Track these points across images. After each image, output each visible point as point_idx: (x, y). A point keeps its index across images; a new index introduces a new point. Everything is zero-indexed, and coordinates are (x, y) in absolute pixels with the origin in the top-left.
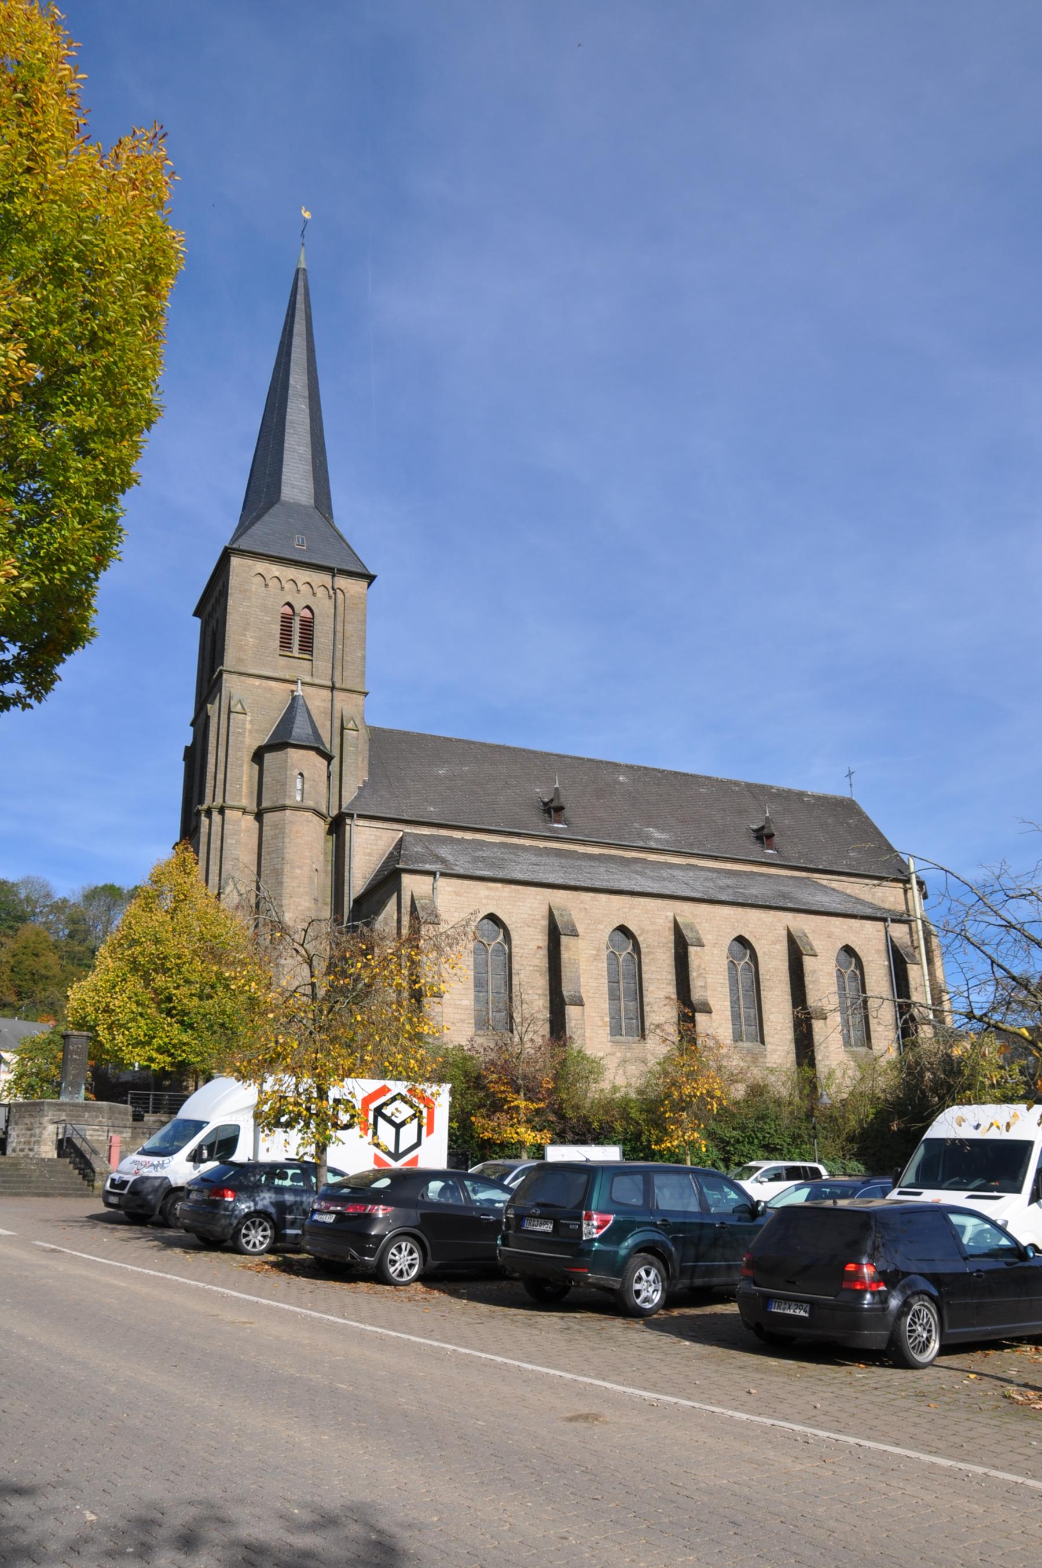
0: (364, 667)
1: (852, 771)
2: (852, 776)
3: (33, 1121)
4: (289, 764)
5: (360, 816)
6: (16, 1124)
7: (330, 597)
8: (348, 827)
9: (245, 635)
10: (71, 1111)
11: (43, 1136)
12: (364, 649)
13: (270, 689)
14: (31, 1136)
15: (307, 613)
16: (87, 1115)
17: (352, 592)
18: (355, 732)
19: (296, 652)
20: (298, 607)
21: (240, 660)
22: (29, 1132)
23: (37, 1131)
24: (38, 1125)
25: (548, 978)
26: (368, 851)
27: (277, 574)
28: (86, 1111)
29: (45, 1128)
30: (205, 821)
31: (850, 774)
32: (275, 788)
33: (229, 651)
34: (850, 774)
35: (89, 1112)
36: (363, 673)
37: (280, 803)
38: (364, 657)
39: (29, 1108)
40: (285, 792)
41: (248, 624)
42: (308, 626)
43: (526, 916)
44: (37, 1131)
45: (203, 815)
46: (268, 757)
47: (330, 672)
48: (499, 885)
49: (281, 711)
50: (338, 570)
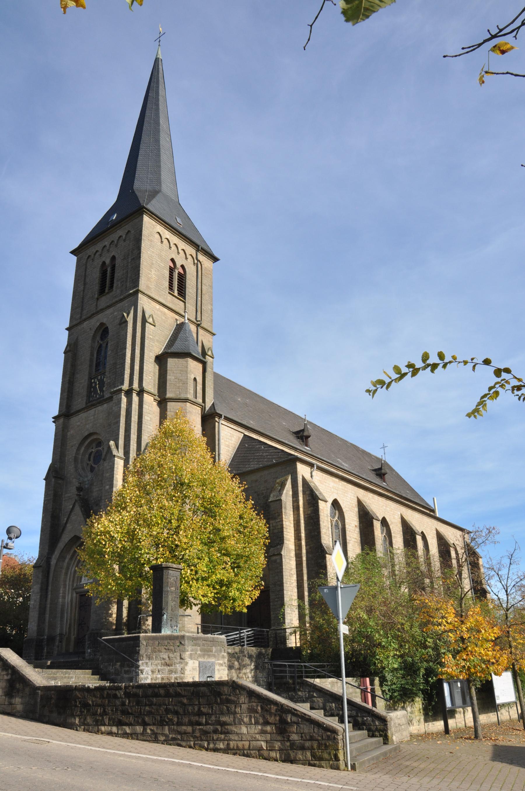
0: (212, 316)
1: (385, 445)
2: (386, 449)
3: (171, 655)
4: (189, 370)
5: (227, 419)
6: (149, 658)
7: (194, 264)
8: (217, 424)
9: (151, 271)
10: (204, 645)
11: (186, 672)
12: (212, 305)
13: (165, 314)
14: (171, 672)
15: (182, 271)
16: (214, 649)
17: (206, 266)
18: (211, 359)
19: (176, 293)
20: (178, 265)
21: (148, 287)
22: (167, 668)
23: (178, 667)
24: (179, 660)
25: (360, 547)
26: (227, 443)
27: (168, 237)
28: (214, 645)
29: (187, 664)
30: (124, 399)
31: (384, 447)
32: (178, 385)
33: (142, 278)
34: (384, 447)
35: (215, 646)
36: (212, 321)
37: (183, 396)
38: (212, 311)
39: (166, 642)
40: (187, 389)
41: (153, 264)
42: (182, 278)
43: (349, 503)
44: (178, 667)
45: (123, 394)
46: (171, 362)
47: (195, 314)
48: (337, 480)
49: (171, 331)
50: (201, 248)
